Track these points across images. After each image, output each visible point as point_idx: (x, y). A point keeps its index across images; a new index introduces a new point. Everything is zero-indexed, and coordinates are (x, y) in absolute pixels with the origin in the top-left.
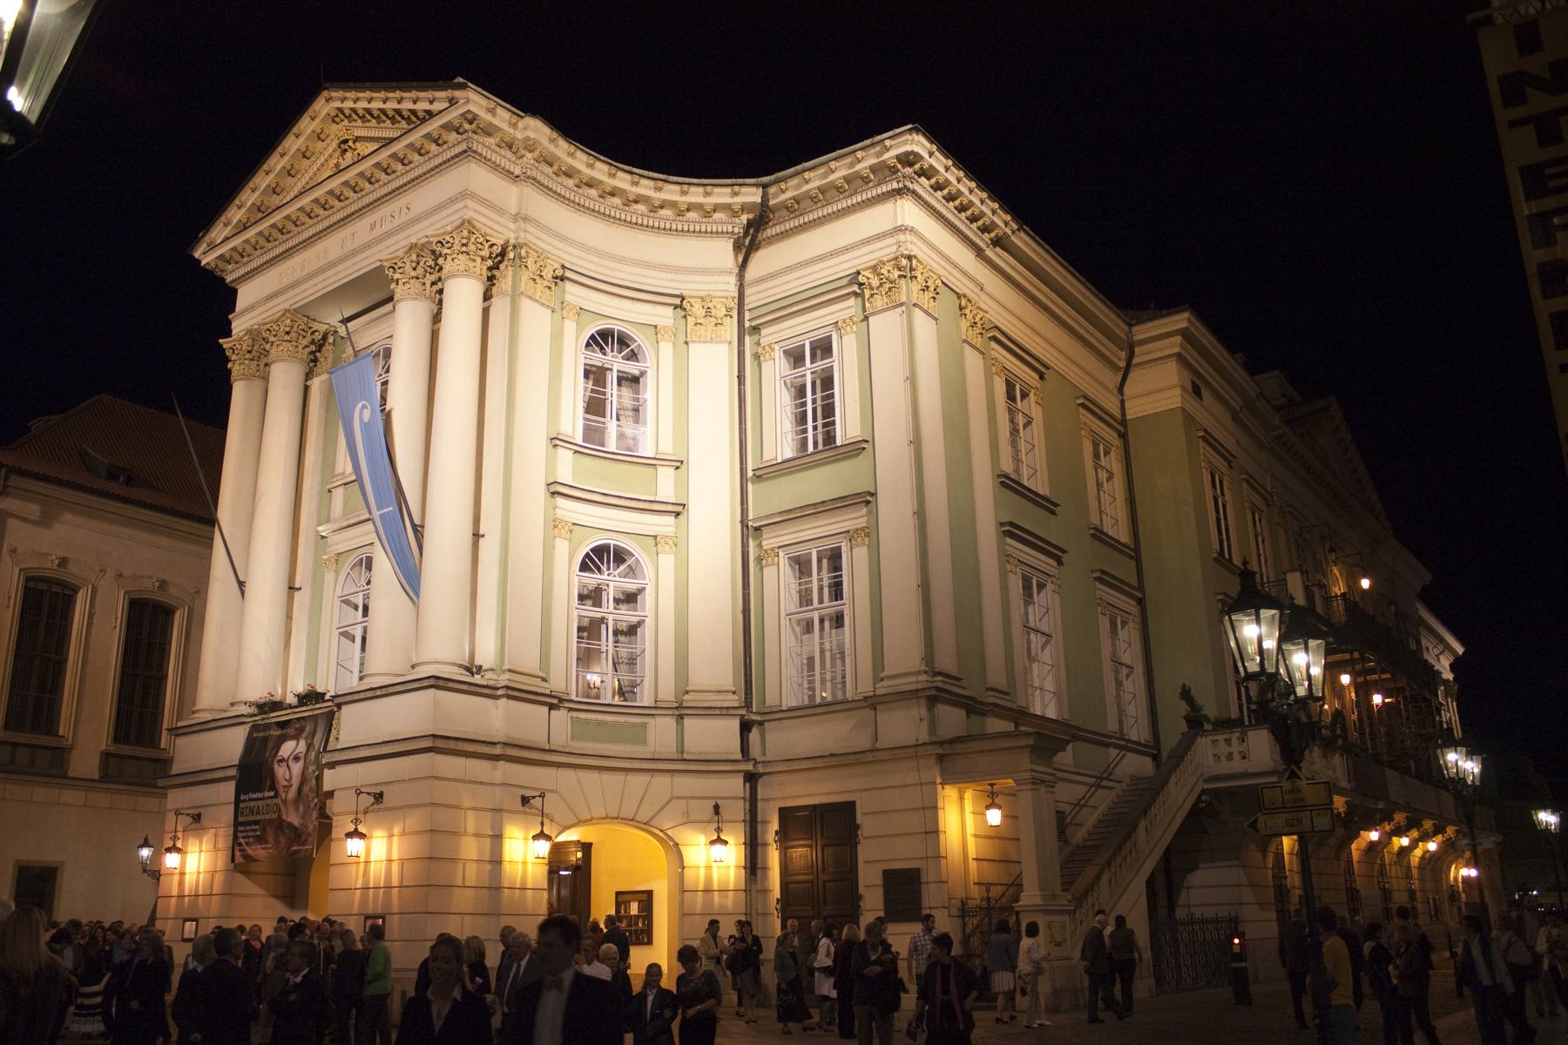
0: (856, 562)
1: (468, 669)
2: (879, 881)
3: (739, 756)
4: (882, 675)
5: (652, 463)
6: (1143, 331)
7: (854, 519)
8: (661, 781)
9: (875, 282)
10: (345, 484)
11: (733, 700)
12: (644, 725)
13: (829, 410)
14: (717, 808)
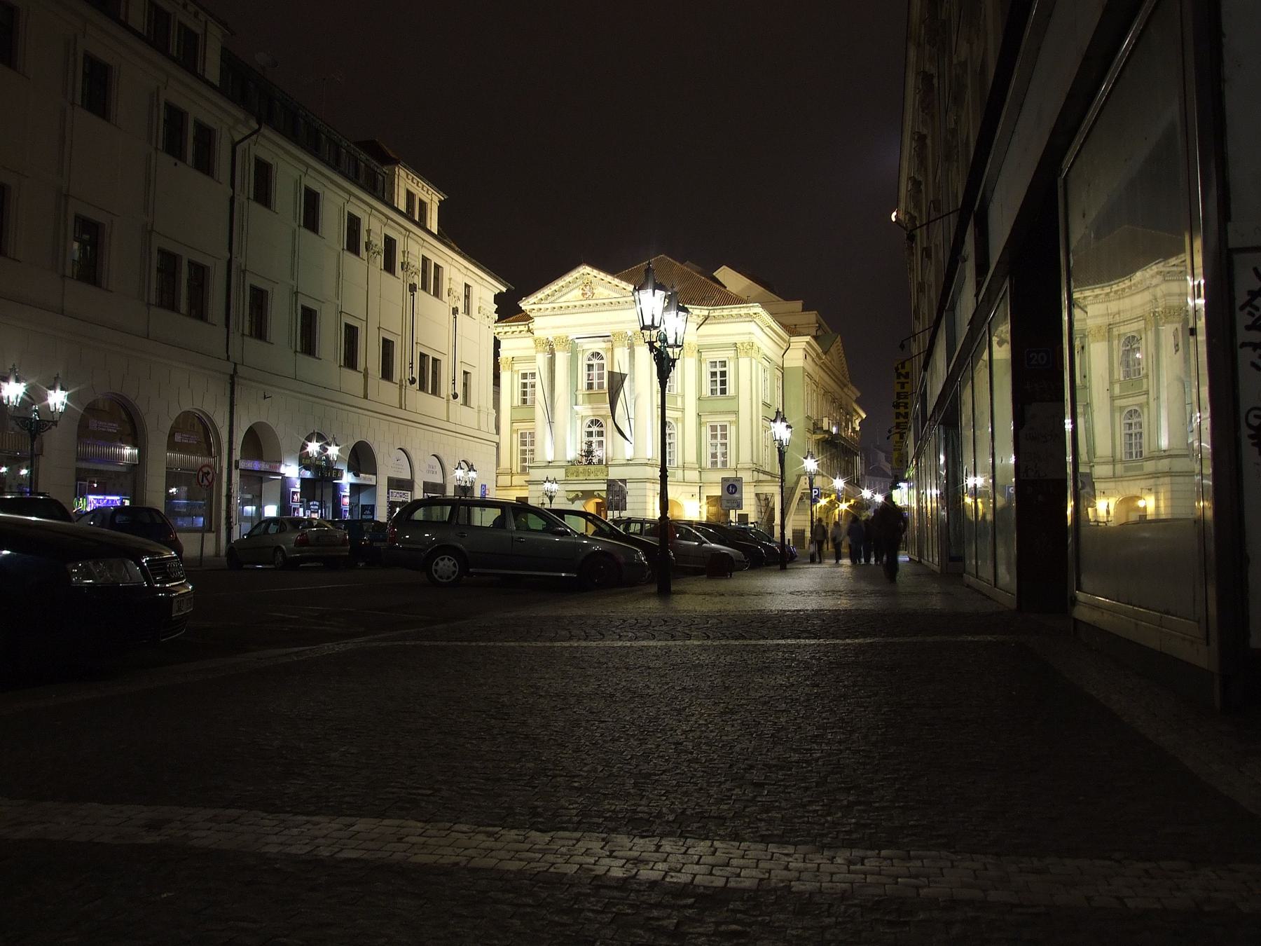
0: (731, 431)
6: (793, 339)
7: (732, 418)
9: (742, 348)
11: (697, 466)
12: (675, 473)
13: (723, 383)
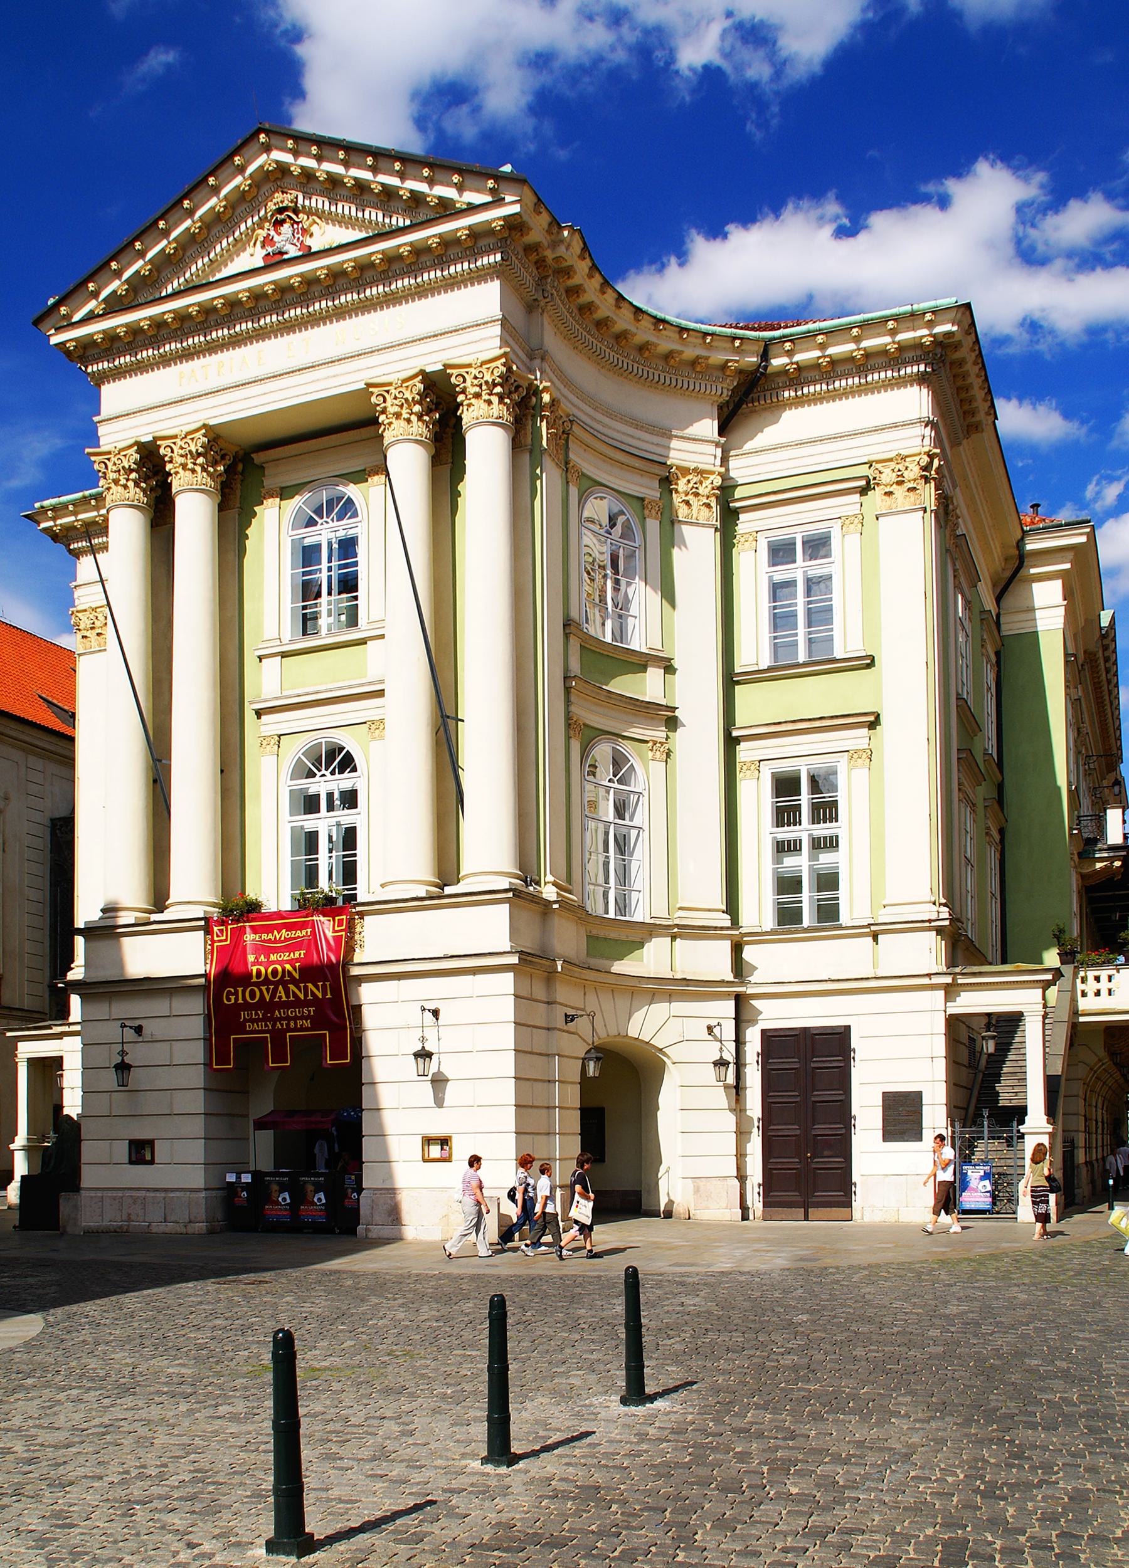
3: (730, 977)
7: (858, 738)
10: (284, 655)
13: (819, 616)
14: (710, 1029)
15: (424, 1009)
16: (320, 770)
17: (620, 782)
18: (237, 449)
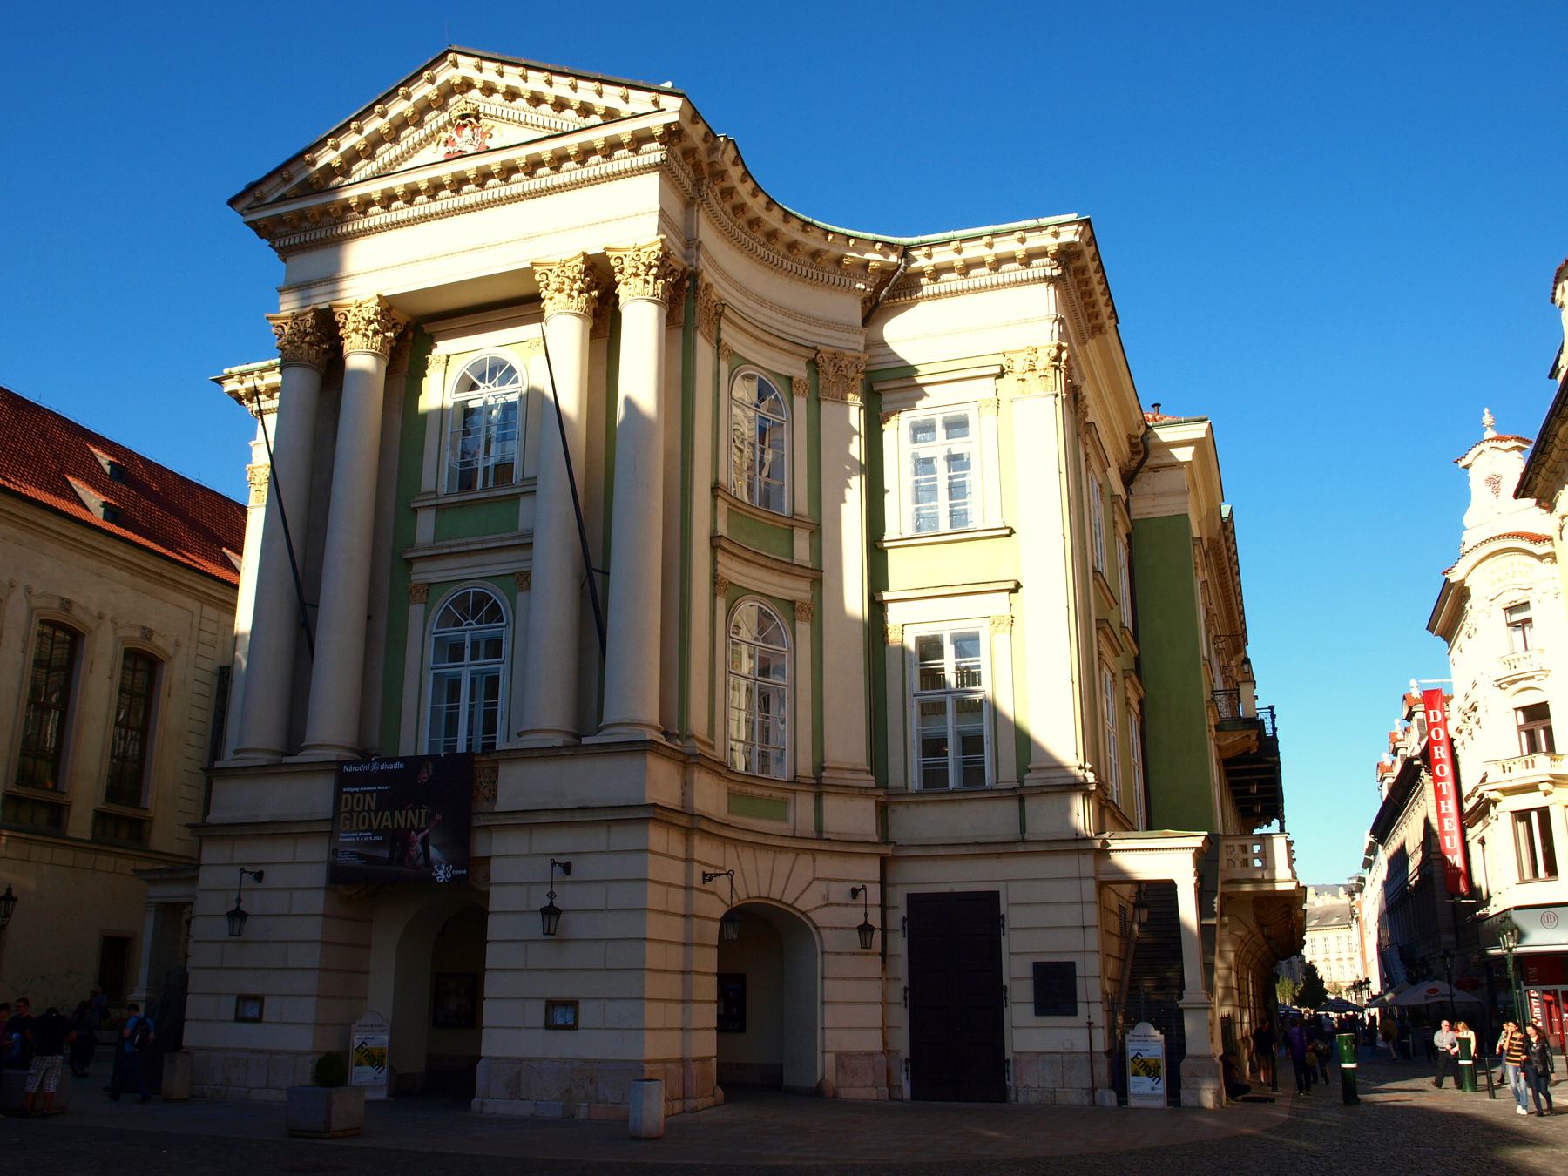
1: (665, 733)
2: (1029, 972)
3: (876, 839)
4: (1029, 766)
5: (791, 524)
8: (804, 861)
10: (439, 508)
12: (785, 802)
14: (855, 893)
15: (555, 863)
16: (466, 619)
17: (765, 640)
18: (409, 319)
